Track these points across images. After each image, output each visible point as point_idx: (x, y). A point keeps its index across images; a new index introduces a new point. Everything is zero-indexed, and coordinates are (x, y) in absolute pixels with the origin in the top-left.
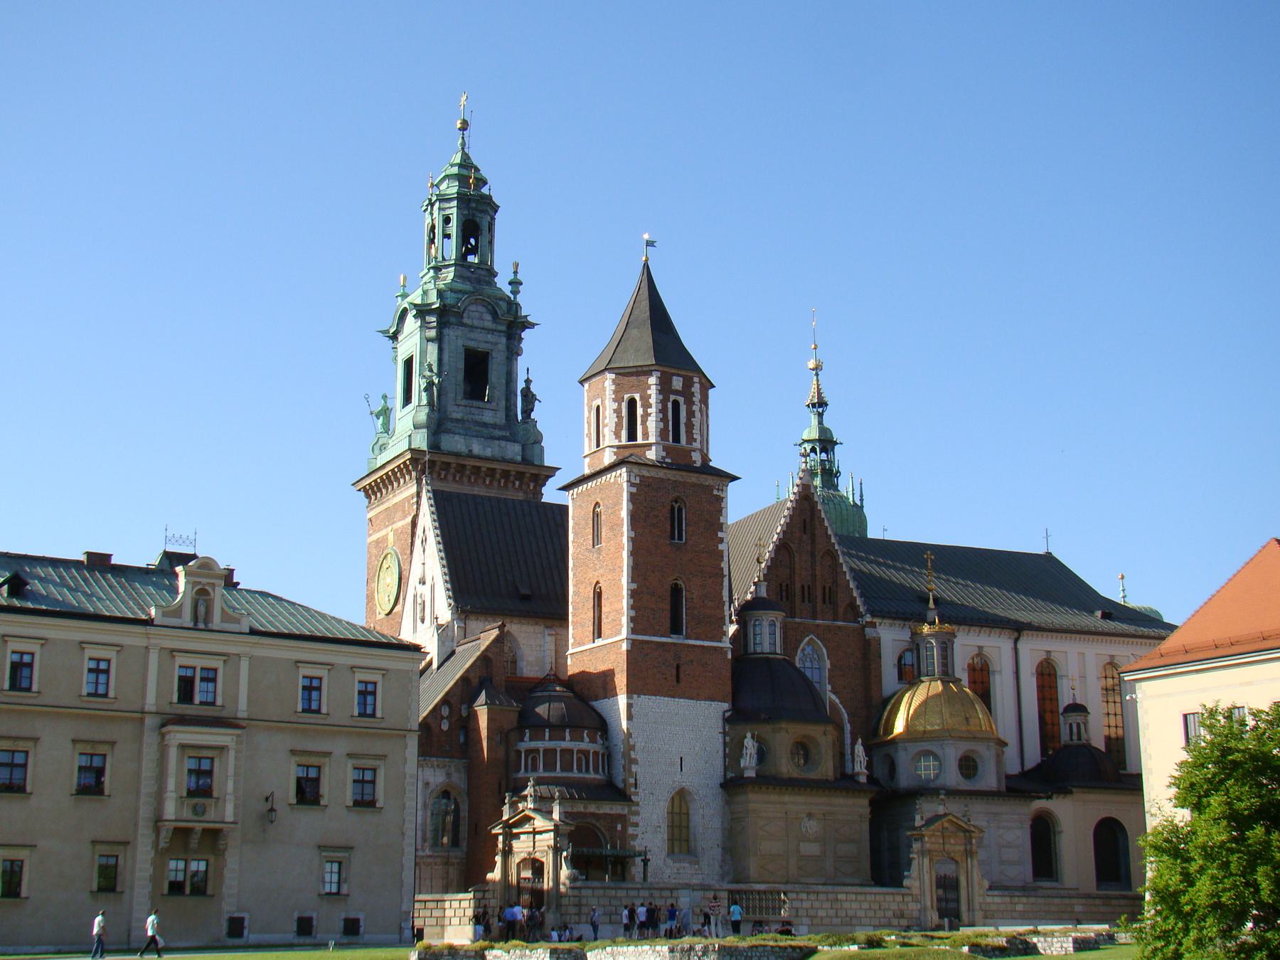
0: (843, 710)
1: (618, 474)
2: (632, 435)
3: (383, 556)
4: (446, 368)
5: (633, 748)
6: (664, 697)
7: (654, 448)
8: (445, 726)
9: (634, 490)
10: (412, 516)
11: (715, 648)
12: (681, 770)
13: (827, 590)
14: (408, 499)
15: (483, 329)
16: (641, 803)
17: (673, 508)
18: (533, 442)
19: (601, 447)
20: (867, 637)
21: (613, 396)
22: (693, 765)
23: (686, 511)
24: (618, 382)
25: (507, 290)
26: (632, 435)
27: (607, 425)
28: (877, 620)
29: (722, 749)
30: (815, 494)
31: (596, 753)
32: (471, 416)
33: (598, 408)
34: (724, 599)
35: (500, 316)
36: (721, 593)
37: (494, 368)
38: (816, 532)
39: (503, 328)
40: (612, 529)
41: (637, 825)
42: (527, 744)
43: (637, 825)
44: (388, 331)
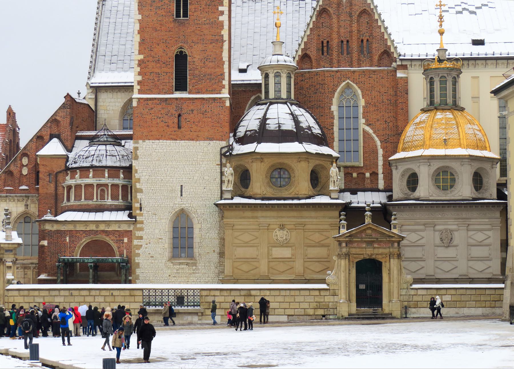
0: (376, 139)
5: (138, 180)
6: (167, 140)
8: (25, 171)
11: (214, 99)
12: (181, 195)
16: (145, 221)
22: (192, 190)
28: (408, 63)
34: (224, 59)
36: (222, 55)
41: (141, 238)
42: (69, 181)
43: (141, 238)
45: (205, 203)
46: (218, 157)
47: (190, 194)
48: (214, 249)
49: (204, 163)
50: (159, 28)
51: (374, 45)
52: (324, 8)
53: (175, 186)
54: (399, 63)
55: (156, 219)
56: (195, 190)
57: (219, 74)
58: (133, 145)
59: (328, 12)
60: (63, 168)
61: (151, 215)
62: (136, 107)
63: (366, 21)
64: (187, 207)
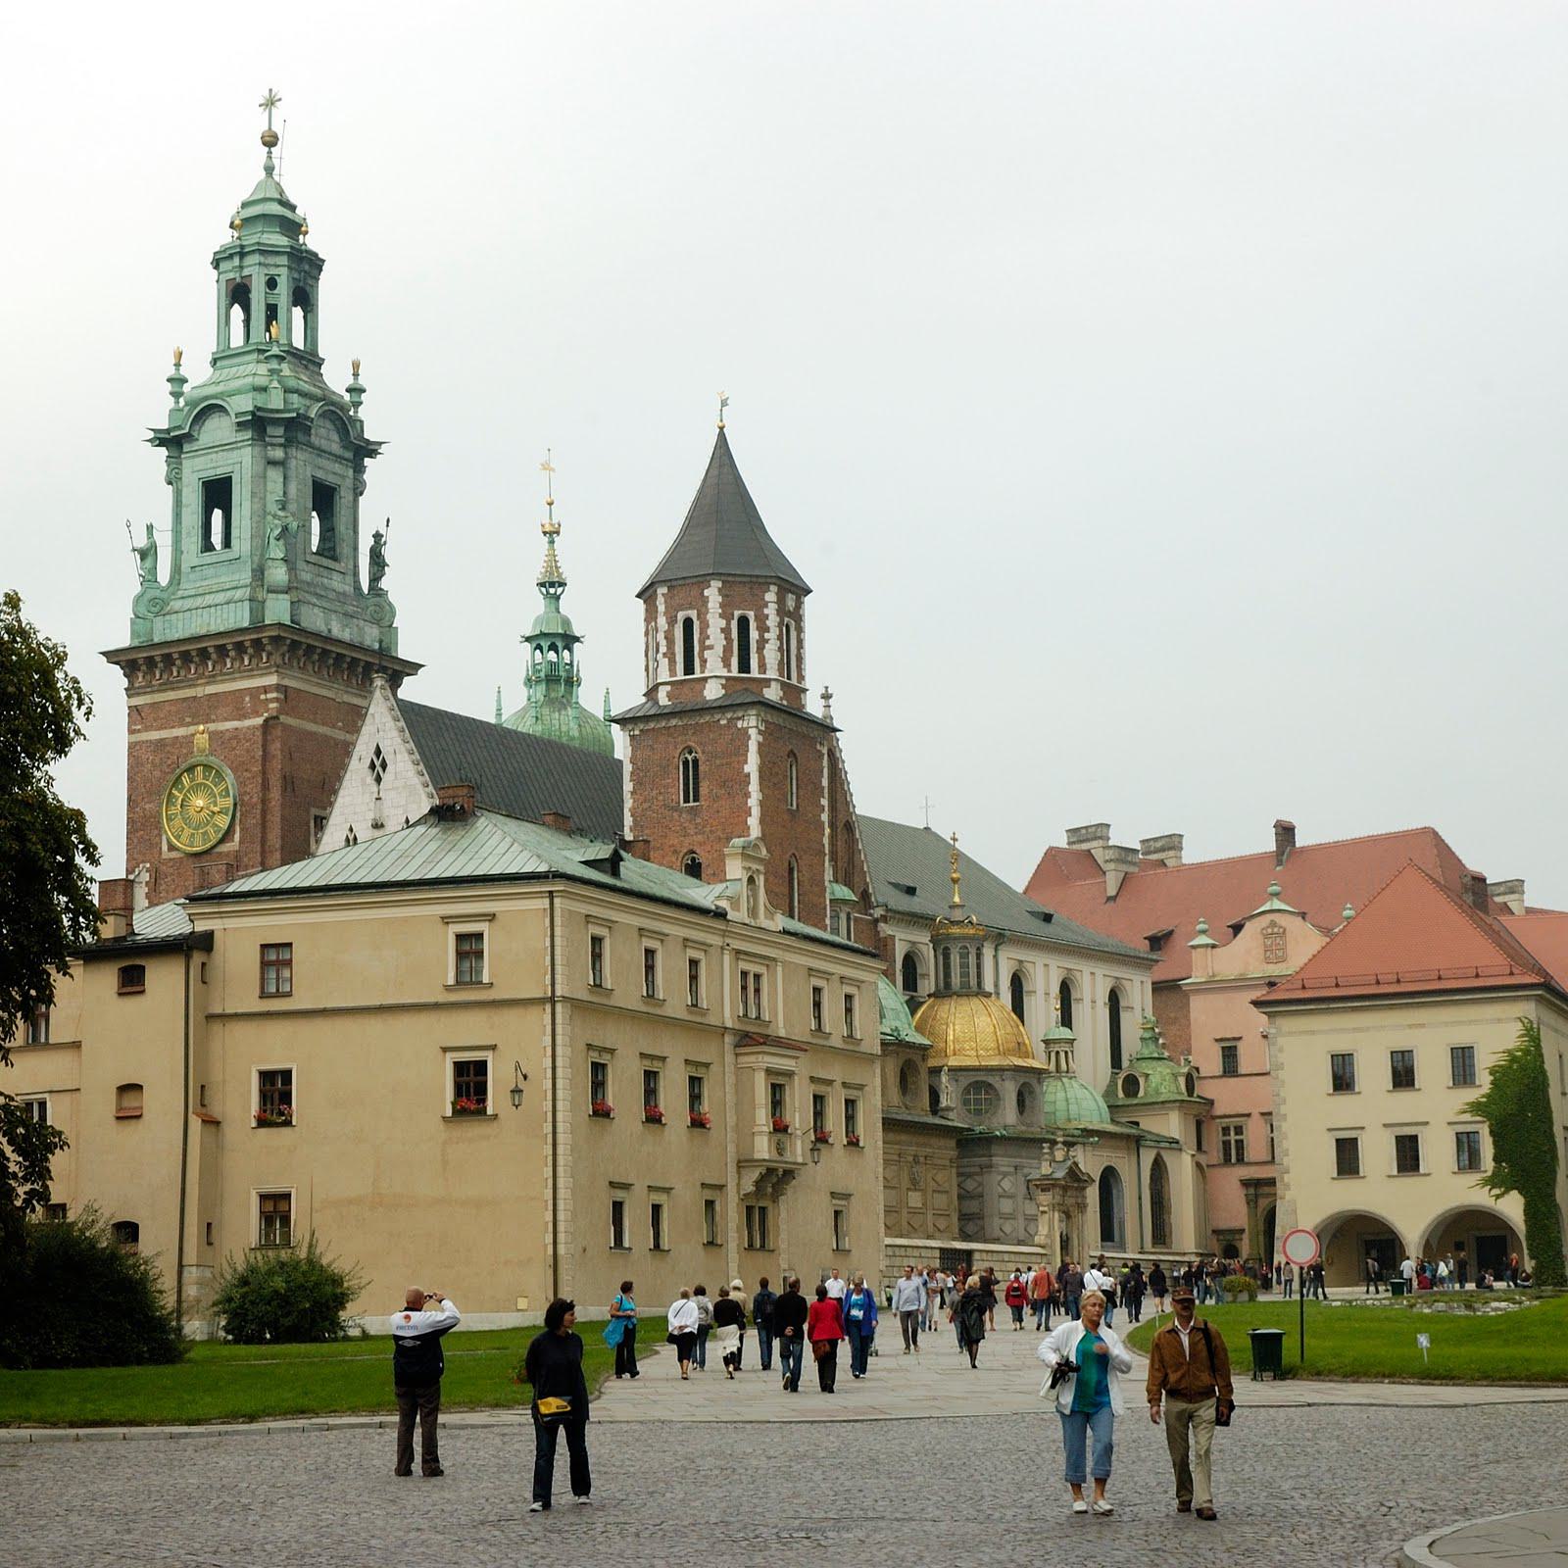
1: (740, 715)
2: (744, 666)
3: (184, 766)
7: (773, 684)
9: (761, 739)
10: (263, 718)
14: (254, 693)
15: (330, 454)
19: (697, 675)
25: (347, 397)
26: (744, 666)
27: (711, 647)
32: (320, 579)
33: (688, 623)
40: (723, 785)
44: (168, 431)
51: (856, 879)
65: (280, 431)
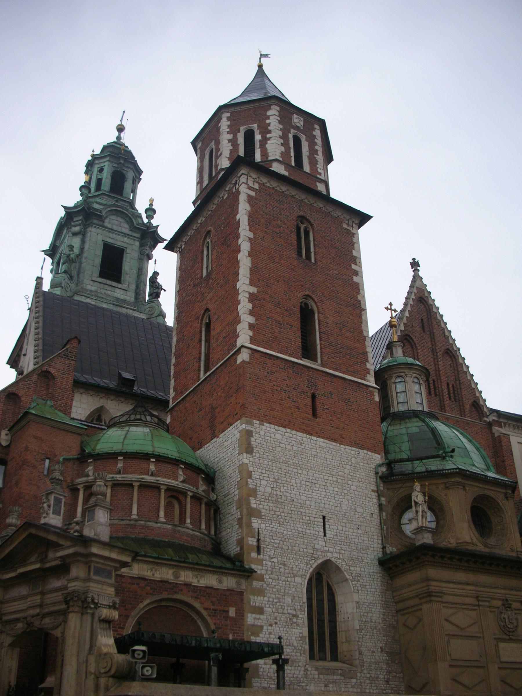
1: (233, 182)
4: (85, 255)
5: (254, 493)
12: (325, 535)
13: (451, 386)
16: (267, 576)
17: (298, 229)
18: (157, 315)
20: (496, 435)
21: (228, 130)
23: (313, 234)
24: (232, 118)
29: (377, 511)
30: (429, 298)
31: (196, 498)
32: (104, 291)
35: (135, 224)
37: (128, 260)
38: (435, 331)
39: (138, 235)
41: (260, 611)
43: (260, 611)
45: (361, 555)
46: (372, 478)
47: (338, 535)
48: (381, 645)
49: (355, 484)
50: (277, 260)
51: (464, 393)
52: (407, 335)
53: (313, 515)
54: (493, 418)
55: (286, 575)
56: (344, 529)
57: (361, 352)
58: (244, 426)
59: (411, 341)
60: (74, 453)
61: (277, 564)
62: (249, 363)
63: (450, 363)
64: (335, 558)
65: (81, 218)
